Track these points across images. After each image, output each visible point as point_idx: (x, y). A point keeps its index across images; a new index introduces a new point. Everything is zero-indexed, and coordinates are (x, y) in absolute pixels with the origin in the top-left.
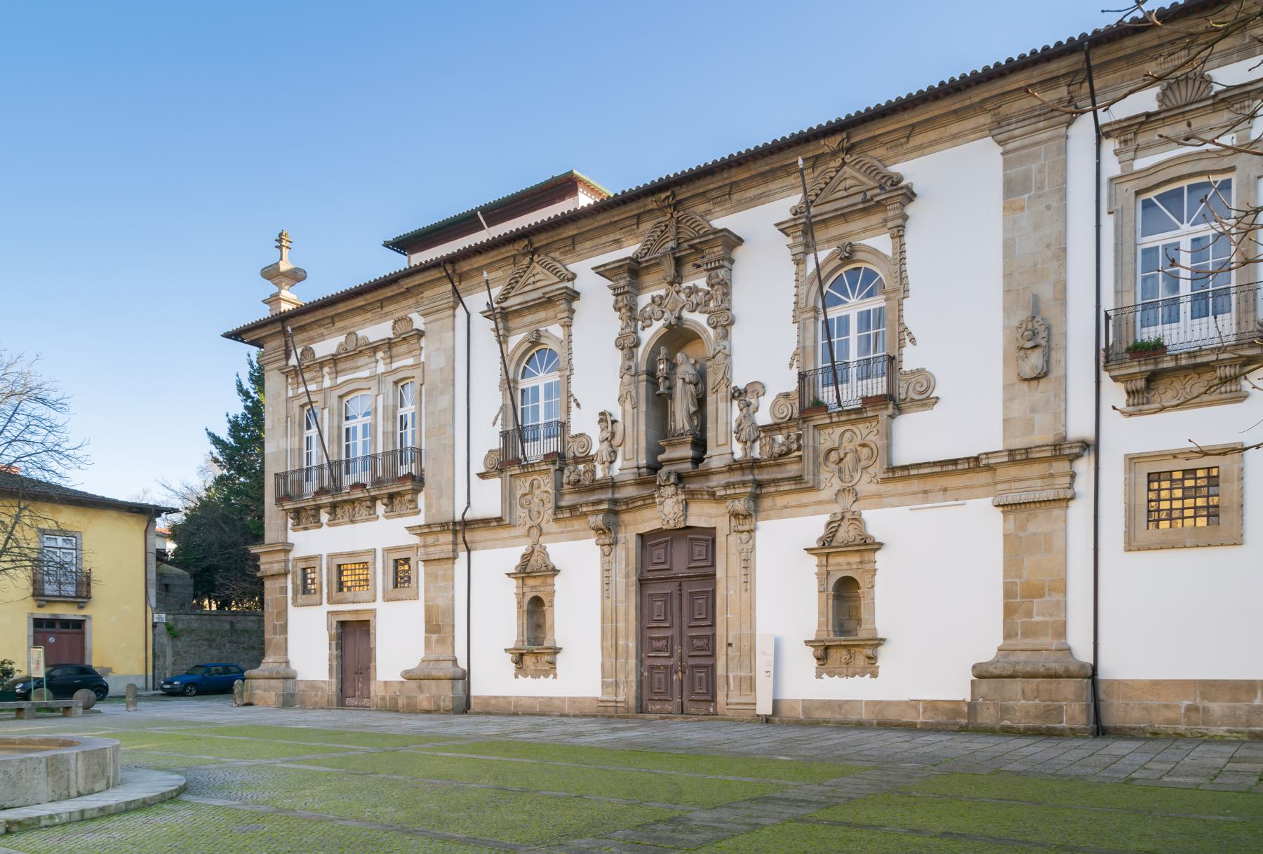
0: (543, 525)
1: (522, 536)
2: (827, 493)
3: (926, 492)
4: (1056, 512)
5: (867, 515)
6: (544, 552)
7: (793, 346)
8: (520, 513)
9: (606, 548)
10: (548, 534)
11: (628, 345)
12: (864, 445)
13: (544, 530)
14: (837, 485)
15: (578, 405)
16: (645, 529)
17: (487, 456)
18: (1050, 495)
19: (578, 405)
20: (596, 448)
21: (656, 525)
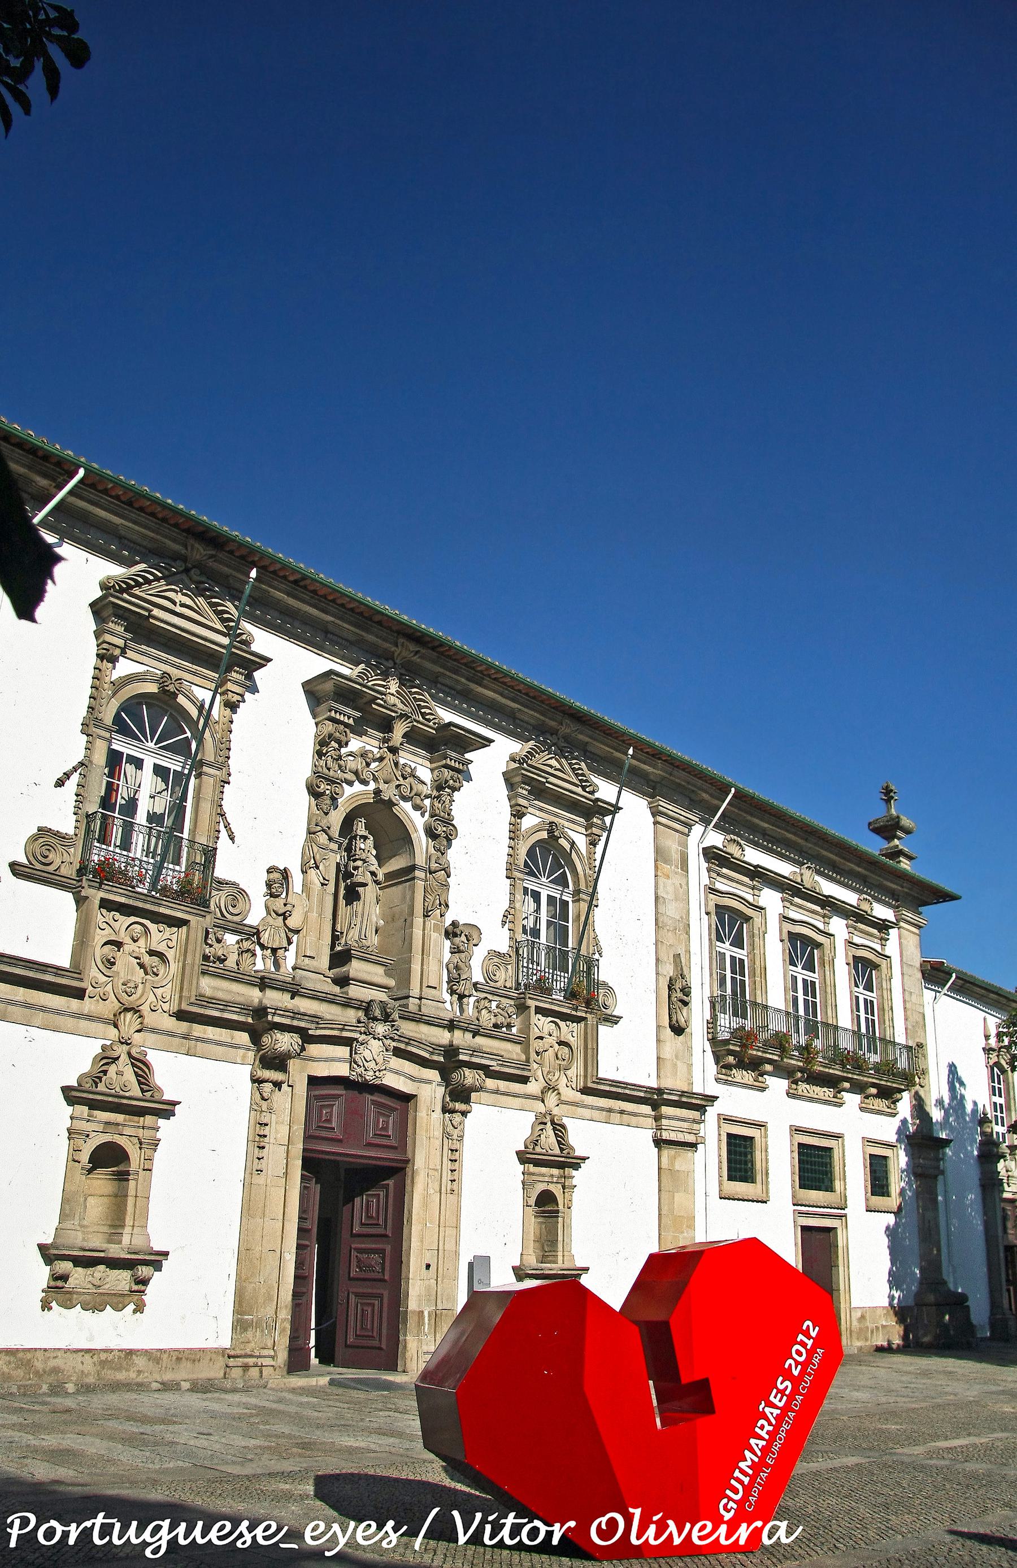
0: (145, 1009)
1: (100, 1019)
2: (533, 1087)
3: (610, 1110)
4: (690, 1154)
5: (566, 1121)
6: (141, 1067)
7: (506, 905)
8: (94, 973)
9: (267, 1087)
10: (154, 1031)
11: (320, 790)
12: (561, 1043)
13: (150, 1019)
14: (542, 1083)
15: (232, 838)
16: (322, 1070)
17: (34, 838)
18: (690, 1138)
19: (232, 838)
20: (255, 917)
21: (342, 1070)
